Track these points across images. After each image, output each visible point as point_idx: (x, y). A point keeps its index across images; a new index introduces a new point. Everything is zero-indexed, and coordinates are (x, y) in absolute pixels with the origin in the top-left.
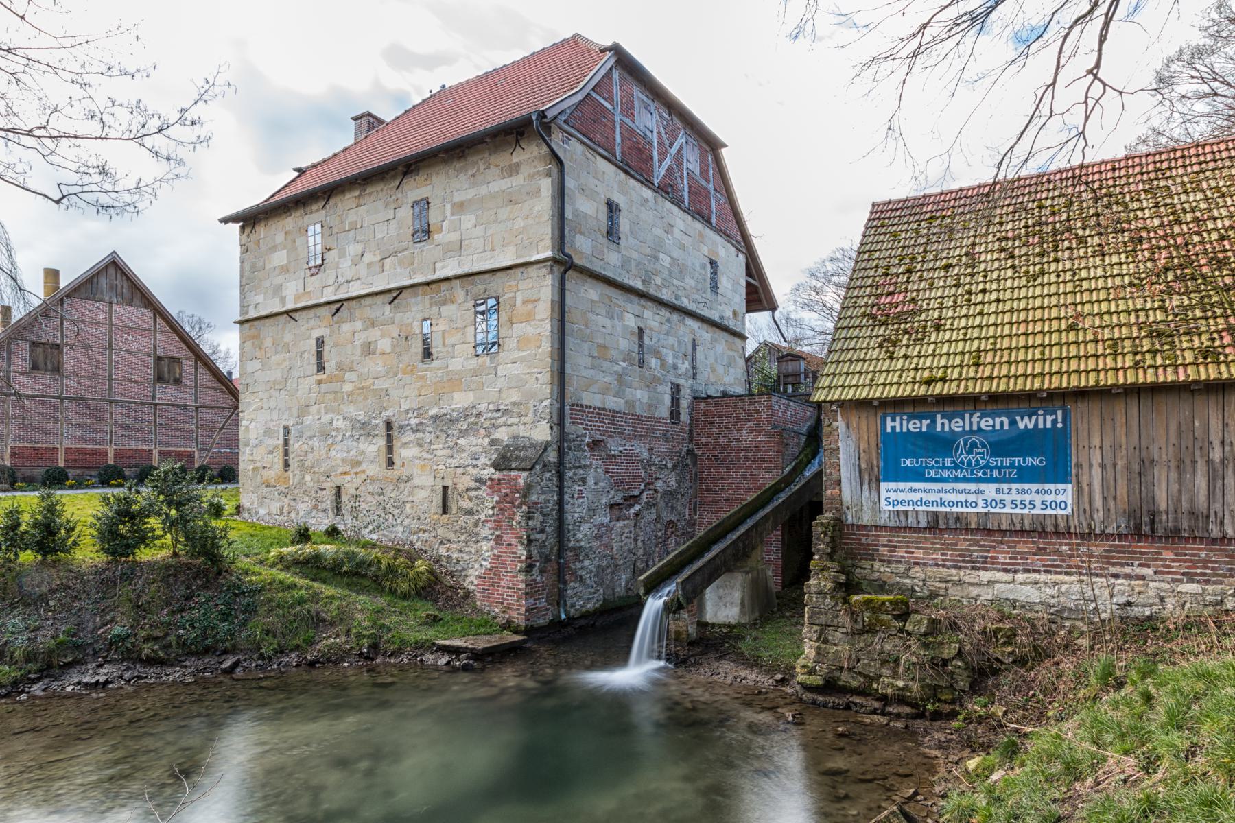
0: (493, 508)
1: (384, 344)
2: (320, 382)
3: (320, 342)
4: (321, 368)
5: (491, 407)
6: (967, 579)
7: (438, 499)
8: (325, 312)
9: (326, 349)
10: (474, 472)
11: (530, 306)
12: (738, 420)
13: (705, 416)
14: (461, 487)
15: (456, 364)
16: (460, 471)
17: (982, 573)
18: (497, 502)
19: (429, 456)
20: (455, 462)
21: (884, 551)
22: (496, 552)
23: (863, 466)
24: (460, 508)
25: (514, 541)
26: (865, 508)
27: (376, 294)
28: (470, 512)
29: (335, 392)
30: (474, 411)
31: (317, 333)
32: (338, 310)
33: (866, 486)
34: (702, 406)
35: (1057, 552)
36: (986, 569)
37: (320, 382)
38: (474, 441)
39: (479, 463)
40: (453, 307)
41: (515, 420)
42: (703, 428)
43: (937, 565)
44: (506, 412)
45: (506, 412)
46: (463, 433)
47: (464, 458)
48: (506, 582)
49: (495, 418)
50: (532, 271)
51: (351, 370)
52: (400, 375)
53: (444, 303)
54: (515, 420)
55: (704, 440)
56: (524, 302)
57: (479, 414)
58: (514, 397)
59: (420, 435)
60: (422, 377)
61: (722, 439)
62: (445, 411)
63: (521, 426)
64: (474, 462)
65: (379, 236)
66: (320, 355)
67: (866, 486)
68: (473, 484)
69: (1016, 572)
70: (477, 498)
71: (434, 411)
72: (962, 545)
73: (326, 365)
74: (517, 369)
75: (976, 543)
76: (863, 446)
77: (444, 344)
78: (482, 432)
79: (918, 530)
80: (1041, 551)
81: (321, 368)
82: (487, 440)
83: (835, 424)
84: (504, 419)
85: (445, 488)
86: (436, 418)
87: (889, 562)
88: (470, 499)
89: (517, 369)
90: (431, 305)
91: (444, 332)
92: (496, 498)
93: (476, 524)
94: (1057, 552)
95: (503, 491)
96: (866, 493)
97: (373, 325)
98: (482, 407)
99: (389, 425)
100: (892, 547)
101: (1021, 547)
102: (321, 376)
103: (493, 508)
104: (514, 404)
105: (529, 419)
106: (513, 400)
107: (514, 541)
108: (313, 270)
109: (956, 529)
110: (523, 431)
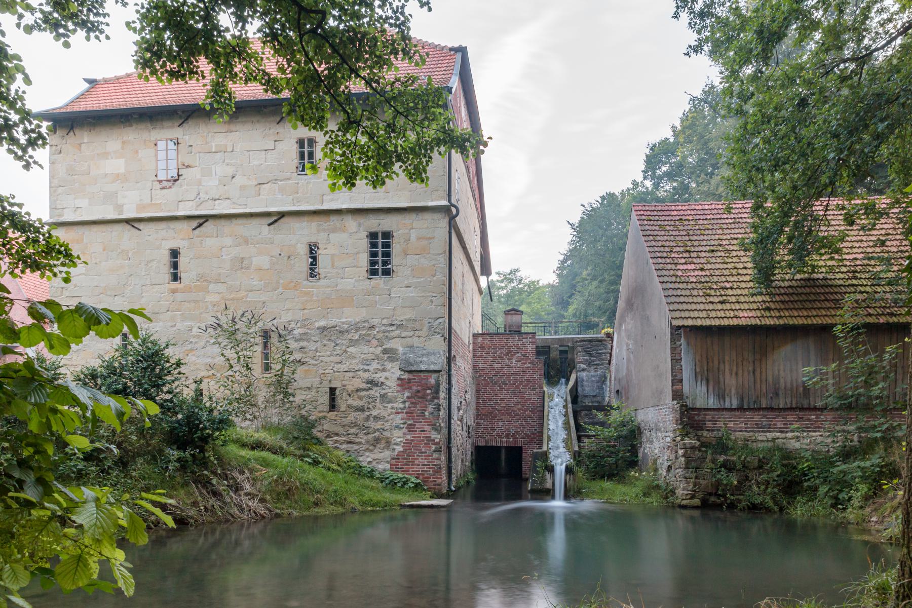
0: (404, 402)
1: (263, 261)
2: (174, 291)
3: (175, 253)
4: (176, 277)
5: (385, 322)
6: (760, 438)
7: (325, 399)
8: (187, 226)
9: (182, 261)
10: (366, 375)
11: (425, 242)
12: (510, 352)
13: (482, 347)
14: (350, 388)
15: (347, 284)
16: (351, 374)
17: (768, 434)
18: (408, 397)
19: (315, 362)
20: (344, 367)
21: (709, 424)
22: (409, 437)
23: (698, 370)
24: (349, 406)
25: (427, 428)
26: (698, 397)
27: (252, 215)
28: (361, 409)
29: (196, 302)
30: (367, 325)
31: (174, 245)
32: (200, 225)
33: (699, 383)
34: (480, 339)
35: (809, 420)
36: (770, 432)
37: (174, 291)
38: (366, 349)
39: (371, 368)
40: (344, 236)
41: (411, 333)
42: (480, 357)
43: (741, 431)
44: (400, 326)
45: (400, 326)
46: (353, 343)
47: (355, 364)
48: (421, 460)
49: (389, 331)
50: (428, 216)
51: (218, 282)
52: (280, 290)
53: (334, 230)
54: (411, 333)
55: (481, 366)
56: (419, 239)
57: (373, 327)
58: (409, 314)
59: (304, 344)
60: (307, 294)
61: (496, 366)
62: (334, 323)
63: (415, 339)
64: (366, 367)
65: (256, 163)
66: (175, 266)
67: (699, 383)
68: (364, 386)
69: (787, 432)
70: (369, 397)
71: (322, 323)
72: (757, 418)
73: (183, 275)
74: (412, 293)
75: (765, 416)
76: (698, 357)
77: (333, 266)
78: (375, 342)
79: (731, 410)
80: (800, 419)
81: (176, 277)
82: (380, 349)
83: (678, 343)
84: (398, 332)
85: (333, 391)
86: (323, 329)
87: (713, 431)
88: (361, 398)
89: (412, 293)
90: (318, 231)
91: (333, 255)
92: (407, 394)
93: (367, 419)
94: (809, 420)
95: (414, 388)
96: (699, 388)
97: (246, 242)
98: (375, 322)
99: (266, 335)
100: (715, 421)
101: (790, 418)
102: (175, 285)
103: (404, 402)
104: (409, 320)
105: (424, 332)
106: (407, 317)
107: (427, 428)
108: (165, 184)
109: (753, 409)
110: (416, 342)
